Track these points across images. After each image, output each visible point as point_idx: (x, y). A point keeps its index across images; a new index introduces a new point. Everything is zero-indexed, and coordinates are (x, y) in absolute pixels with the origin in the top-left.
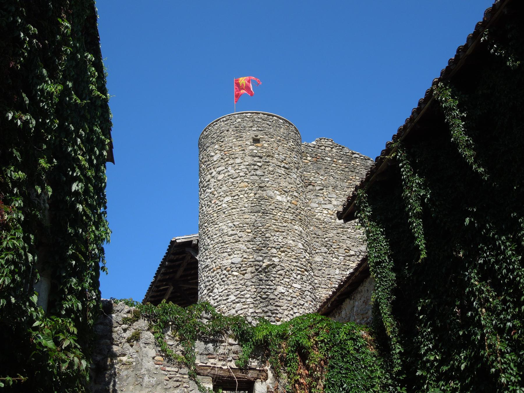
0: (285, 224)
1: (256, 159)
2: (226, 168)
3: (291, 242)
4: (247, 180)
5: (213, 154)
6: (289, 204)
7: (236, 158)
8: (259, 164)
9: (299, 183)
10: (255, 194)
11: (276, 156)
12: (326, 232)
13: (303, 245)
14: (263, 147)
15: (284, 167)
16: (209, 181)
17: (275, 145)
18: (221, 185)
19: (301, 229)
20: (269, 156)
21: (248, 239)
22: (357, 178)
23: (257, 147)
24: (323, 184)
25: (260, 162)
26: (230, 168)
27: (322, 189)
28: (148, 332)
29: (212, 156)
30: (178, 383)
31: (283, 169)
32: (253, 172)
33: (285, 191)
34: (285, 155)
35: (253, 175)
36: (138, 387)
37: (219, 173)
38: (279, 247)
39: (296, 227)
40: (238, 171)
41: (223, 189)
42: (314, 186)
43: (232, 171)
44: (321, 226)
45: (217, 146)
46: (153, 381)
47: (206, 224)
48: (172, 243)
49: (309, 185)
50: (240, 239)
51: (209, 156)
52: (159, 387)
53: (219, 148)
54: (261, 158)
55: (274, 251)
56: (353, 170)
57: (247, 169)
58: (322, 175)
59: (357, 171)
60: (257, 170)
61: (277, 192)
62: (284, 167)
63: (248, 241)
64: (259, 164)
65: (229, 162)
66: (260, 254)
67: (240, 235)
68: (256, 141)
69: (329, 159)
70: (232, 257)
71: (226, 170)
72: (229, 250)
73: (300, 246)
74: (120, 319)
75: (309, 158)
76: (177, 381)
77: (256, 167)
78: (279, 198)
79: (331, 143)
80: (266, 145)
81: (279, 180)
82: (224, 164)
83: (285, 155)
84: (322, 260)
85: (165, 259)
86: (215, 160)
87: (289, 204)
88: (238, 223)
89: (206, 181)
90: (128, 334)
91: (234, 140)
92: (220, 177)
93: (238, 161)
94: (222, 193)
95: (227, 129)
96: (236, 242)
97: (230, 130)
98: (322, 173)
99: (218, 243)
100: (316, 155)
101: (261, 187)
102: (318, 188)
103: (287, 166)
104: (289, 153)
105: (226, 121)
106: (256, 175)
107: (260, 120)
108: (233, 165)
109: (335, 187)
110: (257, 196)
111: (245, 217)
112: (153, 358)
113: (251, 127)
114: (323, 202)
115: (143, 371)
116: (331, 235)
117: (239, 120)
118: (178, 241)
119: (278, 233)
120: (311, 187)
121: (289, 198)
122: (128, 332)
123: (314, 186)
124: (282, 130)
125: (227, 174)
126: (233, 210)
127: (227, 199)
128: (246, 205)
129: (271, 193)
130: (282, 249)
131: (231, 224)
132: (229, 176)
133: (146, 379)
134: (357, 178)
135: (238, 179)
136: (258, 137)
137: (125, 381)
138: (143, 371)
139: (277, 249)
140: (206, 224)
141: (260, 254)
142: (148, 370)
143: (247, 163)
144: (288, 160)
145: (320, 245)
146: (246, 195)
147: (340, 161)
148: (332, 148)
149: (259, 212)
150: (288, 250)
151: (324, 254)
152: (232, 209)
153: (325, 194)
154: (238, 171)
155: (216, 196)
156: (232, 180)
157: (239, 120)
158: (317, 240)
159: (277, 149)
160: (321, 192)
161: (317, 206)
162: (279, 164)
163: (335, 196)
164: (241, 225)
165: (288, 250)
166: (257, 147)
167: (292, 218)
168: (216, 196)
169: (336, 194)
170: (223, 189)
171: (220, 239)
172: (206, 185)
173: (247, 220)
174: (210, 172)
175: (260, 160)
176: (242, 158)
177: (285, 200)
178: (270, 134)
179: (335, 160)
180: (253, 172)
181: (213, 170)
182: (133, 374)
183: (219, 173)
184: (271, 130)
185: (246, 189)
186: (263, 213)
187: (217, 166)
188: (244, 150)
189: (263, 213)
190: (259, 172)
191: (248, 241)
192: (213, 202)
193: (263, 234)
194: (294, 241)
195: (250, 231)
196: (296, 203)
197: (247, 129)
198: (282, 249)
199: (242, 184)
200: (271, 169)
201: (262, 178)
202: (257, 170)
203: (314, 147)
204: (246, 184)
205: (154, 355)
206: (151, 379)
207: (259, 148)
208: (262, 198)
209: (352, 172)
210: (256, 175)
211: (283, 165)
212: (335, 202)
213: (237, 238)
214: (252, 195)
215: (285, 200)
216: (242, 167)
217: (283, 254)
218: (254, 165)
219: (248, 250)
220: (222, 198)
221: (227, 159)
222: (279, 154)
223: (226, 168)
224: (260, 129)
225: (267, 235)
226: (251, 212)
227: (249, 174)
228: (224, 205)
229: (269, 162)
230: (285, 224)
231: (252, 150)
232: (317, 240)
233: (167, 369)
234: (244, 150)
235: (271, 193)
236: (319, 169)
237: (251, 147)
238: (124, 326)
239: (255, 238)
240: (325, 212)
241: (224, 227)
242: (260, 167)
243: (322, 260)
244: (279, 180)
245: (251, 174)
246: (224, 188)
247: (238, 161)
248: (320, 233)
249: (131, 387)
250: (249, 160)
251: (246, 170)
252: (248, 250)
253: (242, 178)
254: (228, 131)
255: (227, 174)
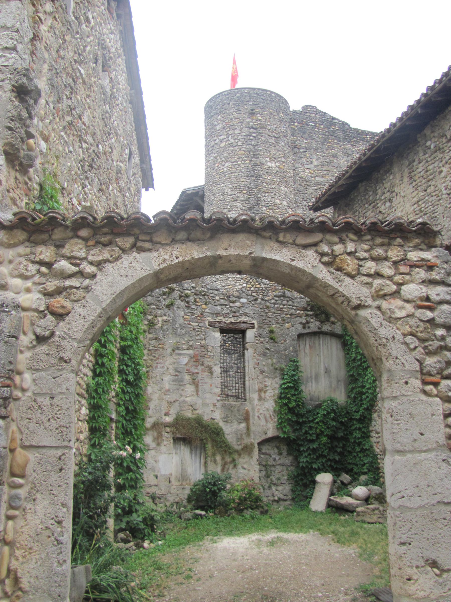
0: (273, 186)
1: (252, 130)
2: (227, 137)
3: (278, 201)
4: (244, 149)
5: (216, 123)
6: (278, 169)
7: (235, 129)
8: (254, 135)
9: (286, 149)
10: (250, 161)
11: (268, 127)
12: (307, 188)
13: (287, 203)
14: (257, 120)
15: (274, 137)
16: (213, 146)
17: (268, 117)
18: (223, 152)
19: (286, 189)
20: (262, 128)
21: (244, 199)
22: (335, 141)
23: (253, 119)
24: (306, 147)
25: (254, 133)
26: (230, 138)
27: (306, 152)
28: (179, 301)
29: (216, 125)
30: (199, 333)
31: (274, 138)
32: (249, 142)
33: (275, 158)
34: (276, 126)
35: (249, 145)
36: (174, 336)
37: (221, 141)
38: (268, 205)
39: (282, 188)
40: (236, 141)
41: (225, 155)
42: (299, 149)
43: (232, 141)
44: (302, 184)
45: (219, 117)
46: (183, 331)
47: (211, 183)
48: (183, 193)
49: (295, 147)
50: (238, 199)
51: (213, 124)
52: (187, 335)
53: (222, 119)
54: (256, 129)
55: (264, 208)
56: (332, 133)
57: (244, 139)
58: (306, 139)
59: (336, 135)
60: (252, 140)
61: (268, 159)
62: (274, 137)
63: (244, 201)
64: (254, 135)
65: (230, 132)
66: (253, 211)
67: (237, 195)
68: (252, 114)
69: (313, 124)
70: (231, 212)
71: (227, 139)
72: (229, 207)
73: (285, 203)
74: (161, 292)
75: (296, 124)
76: (198, 331)
77: (251, 138)
78: (269, 164)
79: (315, 110)
80: (260, 118)
81: (269, 149)
82: (225, 133)
83: (276, 126)
84: (302, 212)
85: (177, 203)
86: (218, 129)
87: (278, 169)
88: (236, 185)
89: (212, 145)
90: (167, 302)
91: (234, 113)
92: (223, 145)
93: (237, 132)
94: (223, 159)
95: (228, 101)
96: (234, 201)
97: (231, 103)
98: (306, 136)
99: (220, 200)
100: (302, 121)
101: (254, 155)
102: (302, 150)
103: (276, 136)
104: (279, 123)
105: (227, 94)
106: (251, 145)
107: (255, 95)
108: (233, 135)
109: (316, 150)
110: (252, 162)
111: (242, 180)
112: (183, 317)
113: (248, 101)
114: (305, 163)
115: (177, 325)
116: (311, 191)
117: (238, 95)
118: (188, 192)
119: (267, 194)
120: (296, 150)
121: (277, 164)
122: (167, 301)
123: (299, 149)
124: (274, 103)
125: (227, 143)
126: (233, 174)
127: (227, 164)
128: (243, 171)
129: (263, 160)
130: (270, 207)
131: (230, 186)
132: (229, 144)
133: (179, 330)
134: (335, 141)
135: (237, 147)
136: (254, 112)
137: (167, 331)
138: (177, 325)
139: (266, 207)
140: (211, 183)
141: (253, 211)
142: (180, 325)
143: (244, 134)
144: (278, 130)
145: (301, 200)
146: (243, 162)
147: (322, 126)
148: (316, 114)
149: (252, 176)
150: (276, 208)
151: (304, 207)
152: (232, 173)
153: (308, 155)
154: (236, 141)
155: (219, 161)
156: (232, 148)
157: (238, 95)
158: (299, 195)
159: (269, 121)
160: (305, 153)
161: (300, 166)
162: (270, 134)
163: (315, 157)
164: (239, 187)
165: (276, 208)
166: (253, 119)
167: (279, 180)
168: (219, 161)
169: (317, 155)
170: (225, 155)
171: (222, 197)
172: (211, 149)
173: (244, 183)
174: (215, 139)
175: (255, 131)
176: (241, 130)
177: (274, 165)
178: (264, 108)
179: (317, 125)
180: (249, 142)
181: (216, 138)
182: (171, 328)
183: (221, 141)
184: (265, 104)
185: (243, 156)
186: (256, 177)
187: (219, 134)
188: (242, 122)
189: (256, 177)
190: (253, 142)
191: (244, 201)
192: (216, 165)
193: (255, 196)
194: (279, 200)
195: (245, 192)
196: (283, 167)
197: (245, 103)
198: (270, 207)
199: (240, 153)
200: (263, 139)
201: (256, 147)
202: (252, 140)
203: (301, 114)
204: (243, 152)
205: (183, 315)
206: (182, 330)
207: (254, 121)
208: (256, 165)
209: (331, 135)
210: (251, 145)
211: (274, 134)
212: (315, 163)
213: (235, 197)
214: (248, 162)
215: (274, 165)
216: (240, 137)
217: (271, 211)
218: (250, 136)
219: (244, 208)
220: (224, 163)
221: (228, 129)
222: (270, 126)
223: (227, 137)
224: (255, 103)
225: (259, 196)
226: (247, 176)
227: (247, 143)
228: (225, 169)
229: (262, 133)
230: (273, 186)
231: (249, 122)
232: (299, 195)
233: (192, 324)
234: (242, 122)
235: (263, 160)
236: (305, 133)
237: (248, 120)
238: (164, 297)
239: (249, 198)
240: (307, 171)
241: (225, 188)
242: (255, 137)
243: (302, 212)
244: (269, 149)
245: (247, 143)
246: (225, 155)
247: (237, 132)
248: (301, 189)
249: (171, 335)
250: (246, 131)
251: (243, 140)
252: (244, 208)
253: (240, 147)
254: (229, 104)
255: (227, 143)
